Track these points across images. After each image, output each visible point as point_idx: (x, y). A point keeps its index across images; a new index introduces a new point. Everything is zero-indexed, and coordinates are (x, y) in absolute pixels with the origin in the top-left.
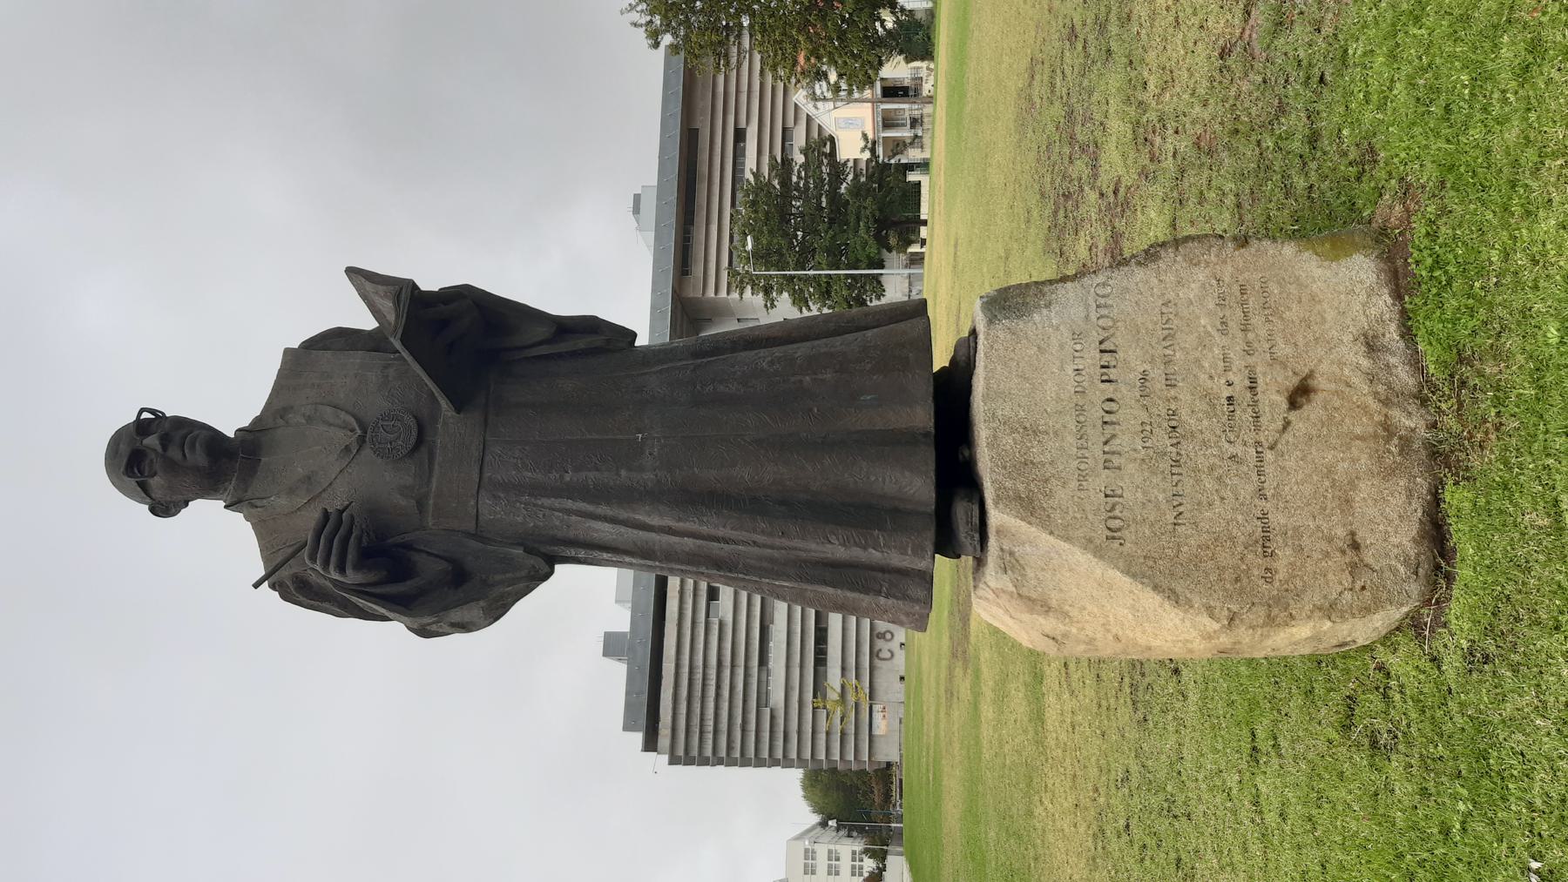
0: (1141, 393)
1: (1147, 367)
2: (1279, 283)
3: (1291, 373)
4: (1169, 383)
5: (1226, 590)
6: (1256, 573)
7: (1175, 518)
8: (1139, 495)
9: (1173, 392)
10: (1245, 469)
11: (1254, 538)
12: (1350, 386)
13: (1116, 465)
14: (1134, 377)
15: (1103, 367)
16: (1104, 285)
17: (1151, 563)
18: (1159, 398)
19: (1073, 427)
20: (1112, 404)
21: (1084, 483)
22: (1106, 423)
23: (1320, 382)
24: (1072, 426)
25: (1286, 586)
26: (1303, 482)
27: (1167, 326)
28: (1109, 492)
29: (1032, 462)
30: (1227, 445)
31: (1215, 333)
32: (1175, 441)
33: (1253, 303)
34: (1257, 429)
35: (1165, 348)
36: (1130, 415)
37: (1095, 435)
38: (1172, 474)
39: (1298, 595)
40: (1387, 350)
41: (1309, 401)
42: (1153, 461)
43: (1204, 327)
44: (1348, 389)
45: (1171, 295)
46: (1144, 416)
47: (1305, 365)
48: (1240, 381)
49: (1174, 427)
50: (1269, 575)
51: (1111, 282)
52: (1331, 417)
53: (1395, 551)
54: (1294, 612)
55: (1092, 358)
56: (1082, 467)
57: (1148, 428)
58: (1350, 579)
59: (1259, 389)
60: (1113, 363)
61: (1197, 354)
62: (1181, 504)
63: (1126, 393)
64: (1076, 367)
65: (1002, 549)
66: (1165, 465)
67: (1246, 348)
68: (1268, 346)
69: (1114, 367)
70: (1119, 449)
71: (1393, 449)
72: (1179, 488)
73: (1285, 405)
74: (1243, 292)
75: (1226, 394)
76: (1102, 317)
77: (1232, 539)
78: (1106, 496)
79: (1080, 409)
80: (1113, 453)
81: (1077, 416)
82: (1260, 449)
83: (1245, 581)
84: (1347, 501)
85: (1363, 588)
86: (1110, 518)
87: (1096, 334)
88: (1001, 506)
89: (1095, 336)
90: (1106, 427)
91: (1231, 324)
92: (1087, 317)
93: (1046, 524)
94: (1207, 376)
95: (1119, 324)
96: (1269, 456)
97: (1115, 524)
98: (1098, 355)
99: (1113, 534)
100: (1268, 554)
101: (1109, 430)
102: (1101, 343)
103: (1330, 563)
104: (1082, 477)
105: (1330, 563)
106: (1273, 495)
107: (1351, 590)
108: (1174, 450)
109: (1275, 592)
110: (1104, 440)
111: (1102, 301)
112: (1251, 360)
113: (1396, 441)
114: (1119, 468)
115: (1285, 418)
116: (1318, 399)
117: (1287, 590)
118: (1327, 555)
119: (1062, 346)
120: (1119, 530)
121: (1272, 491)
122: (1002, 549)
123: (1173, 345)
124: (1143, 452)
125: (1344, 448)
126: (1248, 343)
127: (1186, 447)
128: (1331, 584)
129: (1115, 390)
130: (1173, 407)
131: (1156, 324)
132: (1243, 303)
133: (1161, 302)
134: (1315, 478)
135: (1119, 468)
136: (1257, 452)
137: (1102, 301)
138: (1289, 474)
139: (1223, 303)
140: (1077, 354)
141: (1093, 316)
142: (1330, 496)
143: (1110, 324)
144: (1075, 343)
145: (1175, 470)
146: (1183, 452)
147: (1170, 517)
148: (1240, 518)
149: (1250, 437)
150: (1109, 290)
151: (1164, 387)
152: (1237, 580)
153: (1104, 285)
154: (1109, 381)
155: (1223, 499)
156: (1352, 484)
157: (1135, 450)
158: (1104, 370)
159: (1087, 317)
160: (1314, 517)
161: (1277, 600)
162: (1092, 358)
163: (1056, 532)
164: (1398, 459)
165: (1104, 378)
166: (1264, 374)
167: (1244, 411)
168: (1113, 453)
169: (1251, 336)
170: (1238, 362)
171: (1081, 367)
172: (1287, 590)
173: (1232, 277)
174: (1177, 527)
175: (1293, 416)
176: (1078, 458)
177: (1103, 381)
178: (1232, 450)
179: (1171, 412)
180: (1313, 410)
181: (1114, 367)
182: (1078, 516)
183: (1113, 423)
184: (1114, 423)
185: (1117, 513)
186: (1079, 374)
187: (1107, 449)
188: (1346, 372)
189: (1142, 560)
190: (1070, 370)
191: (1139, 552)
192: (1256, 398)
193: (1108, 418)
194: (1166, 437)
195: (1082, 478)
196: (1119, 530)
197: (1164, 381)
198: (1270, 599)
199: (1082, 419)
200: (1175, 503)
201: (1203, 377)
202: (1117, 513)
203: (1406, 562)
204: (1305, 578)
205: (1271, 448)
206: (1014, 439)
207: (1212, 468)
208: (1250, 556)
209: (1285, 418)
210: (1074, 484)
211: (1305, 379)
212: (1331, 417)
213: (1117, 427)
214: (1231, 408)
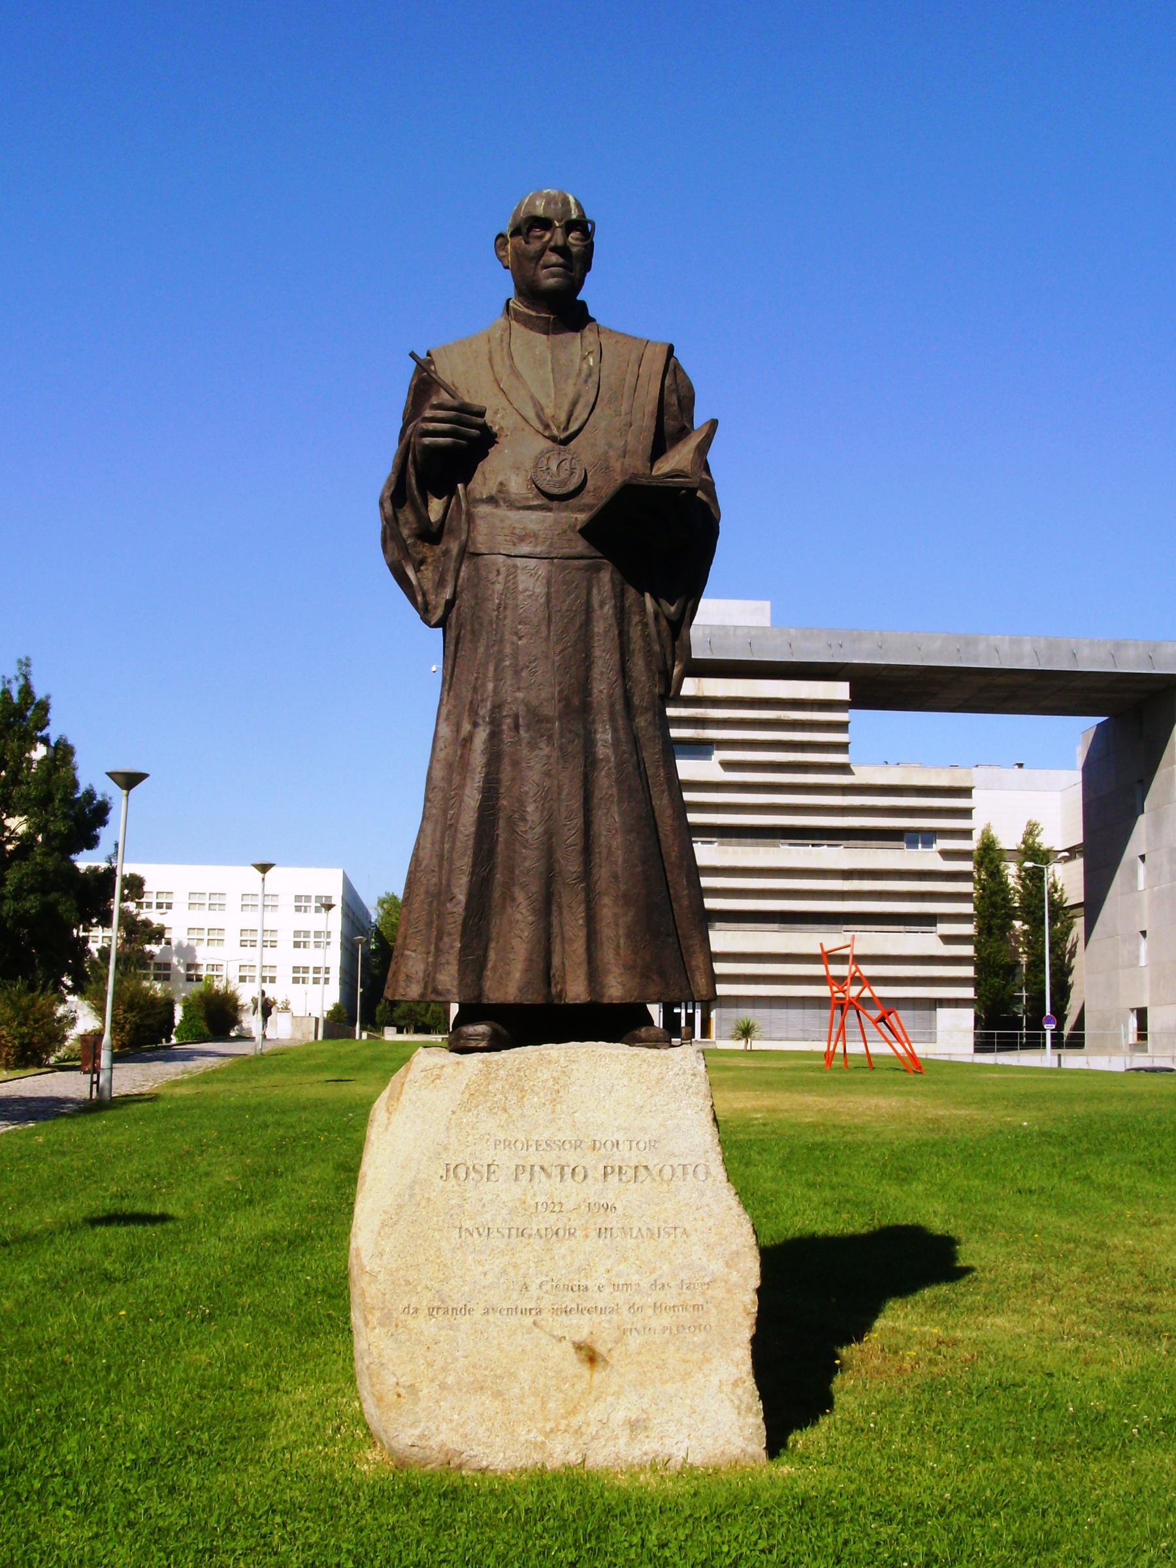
0: (592, 1205)
1: (620, 1210)
2: (704, 1343)
3: (609, 1346)
4: (603, 1230)
5: (397, 1270)
6: (414, 1299)
7: (467, 1229)
8: (489, 1196)
9: (594, 1234)
10: (515, 1296)
11: (447, 1300)
12: (595, 1401)
13: (520, 1177)
14: (610, 1198)
15: (620, 1168)
16: (708, 1173)
17: (423, 1203)
18: (587, 1222)
19: (558, 1138)
20: (582, 1176)
21: (502, 1145)
22: (562, 1168)
23: (599, 1376)
24: (561, 1137)
25: (400, 1325)
26: (501, 1350)
27: (662, 1232)
28: (492, 1168)
29: (523, 1097)
30: (538, 1282)
31: (653, 1277)
32: (543, 1232)
33: (685, 1316)
34: (554, 1311)
35: (640, 1229)
36: (571, 1192)
37: (549, 1158)
38: (509, 1229)
39: (392, 1335)
40: (632, 1439)
41: (581, 1361)
42: (523, 1212)
43: (660, 1268)
44: (593, 1399)
45: (694, 1238)
46: (569, 1205)
47: (618, 1361)
48: (602, 1299)
49: (557, 1233)
50: (411, 1311)
51: (710, 1180)
52: (565, 1380)
53: (433, 1428)
54: (377, 1331)
55: (630, 1158)
56: (519, 1145)
57: (557, 1208)
58: (408, 1384)
59: (594, 1315)
60: (624, 1178)
61: (632, 1260)
62: (480, 1235)
63: (592, 1190)
64: (620, 1142)
65: (443, 1067)
66: (519, 1222)
67: (636, 1307)
68: (639, 1327)
69: (620, 1180)
70: (536, 1180)
71: (532, 1435)
72: (496, 1234)
73: (577, 1338)
74: (696, 1307)
75: (590, 1283)
76: (673, 1170)
77: (446, 1280)
78: (489, 1166)
79: (577, 1145)
80: (532, 1174)
81: (570, 1142)
82: (533, 1312)
83: (407, 1289)
84: (482, 1388)
85: (399, 1396)
86: (468, 1168)
87: (655, 1162)
88: (480, 1066)
89: (653, 1161)
90: (559, 1168)
91: (662, 1293)
92: (673, 1155)
93: (465, 1107)
94: (609, 1267)
95: (665, 1186)
96: (528, 1320)
97: (462, 1172)
98: (633, 1164)
99: (451, 1171)
100: (431, 1312)
101: (556, 1172)
102: (646, 1167)
103: (423, 1367)
104: (508, 1144)
105: (423, 1367)
106: (488, 1321)
107: (397, 1384)
108: (534, 1232)
109: (395, 1315)
110: (545, 1167)
111: (690, 1170)
112: (625, 1309)
113: (541, 1438)
114: (516, 1179)
115: (564, 1338)
116: (585, 1370)
117: (397, 1326)
118: (430, 1365)
119: (643, 1129)
120: (456, 1176)
121: (492, 1320)
122: (443, 1067)
123: (642, 1237)
124: (533, 1203)
125: (533, 1390)
126: (641, 1308)
127: (537, 1243)
128: (403, 1366)
129: (596, 1180)
130: (578, 1233)
131: (665, 1222)
132: (685, 1307)
133: (688, 1228)
134: (505, 1361)
135: (516, 1179)
136: (531, 1310)
137: (690, 1170)
138: (509, 1337)
139: (685, 1287)
140: (634, 1144)
141: (675, 1161)
142: (487, 1373)
143: (666, 1178)
144: (645, 1143)
145: (514, 1232)
146: (532, 1240)
147: (467, 1224)
148: (466, 1288)
149: (546, 1303)
150: (702, 1177)
151: (598, 1226)
152: (408, 1283)
153: (708, 1173)
154: (605, 1174)
155: (485, 1274)
156: (498, 1394)
157: (535, 1195)
158: (617, 1170)
159: (673, 1155)
160: (466, 1357)
161: (388, 1316)
162: (630, 1158)
163: (454, 1117)
164: (522, 1439)
165: (609, 1170)
166: (609, 1322)
167: (573, 1300)
168: (532, 1174)
169: (650, 1311)
170: (621, 1297)
171: (621, 1147)
172: (397, 1326)
173: (712, 1297)
174: (458, 1230)
175: (567, 1346)
176: (527, 1141)
177: (605, 1167)
178: (533, 1288)
179: (572, 1231)
180: (573, 1364)
181: (620, 1180)
182: (470, 1138)
183: (562, 1176)
184: (562, 1176)
185: (472, 1175)
186: (613, 1145)
187: (537, 1168)
188: (610, 1399)
189: (426, 1195)
190: (620, 1136)
191: (435, 1193)
192: (585, 1312)
193: (568, 1171)
194: (547, 1226)
195: (507, 1143)
196: (456, 1176)
197: (605, 1226)
198: (389, 1310)
199: (567, 1146)
200: (481, 1230)
201: (609, 1263)
202: (472, 1175)
203: (422, 1436)
204: (408, 1343)
205: (535, 1323)
206: (547, 1080)
207: (515, 1266)
208: (429, 1295)
209: (564, 1338)
210: (501, 1135)
211: (604, 1360)
212: (565, 1380)
213: (559, 1179)
214: (575, 1289)
